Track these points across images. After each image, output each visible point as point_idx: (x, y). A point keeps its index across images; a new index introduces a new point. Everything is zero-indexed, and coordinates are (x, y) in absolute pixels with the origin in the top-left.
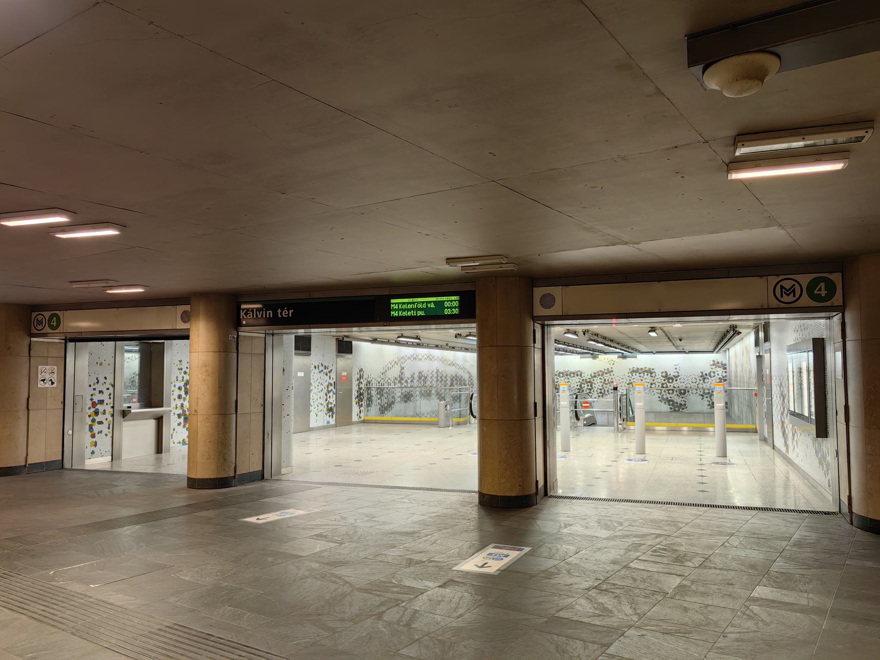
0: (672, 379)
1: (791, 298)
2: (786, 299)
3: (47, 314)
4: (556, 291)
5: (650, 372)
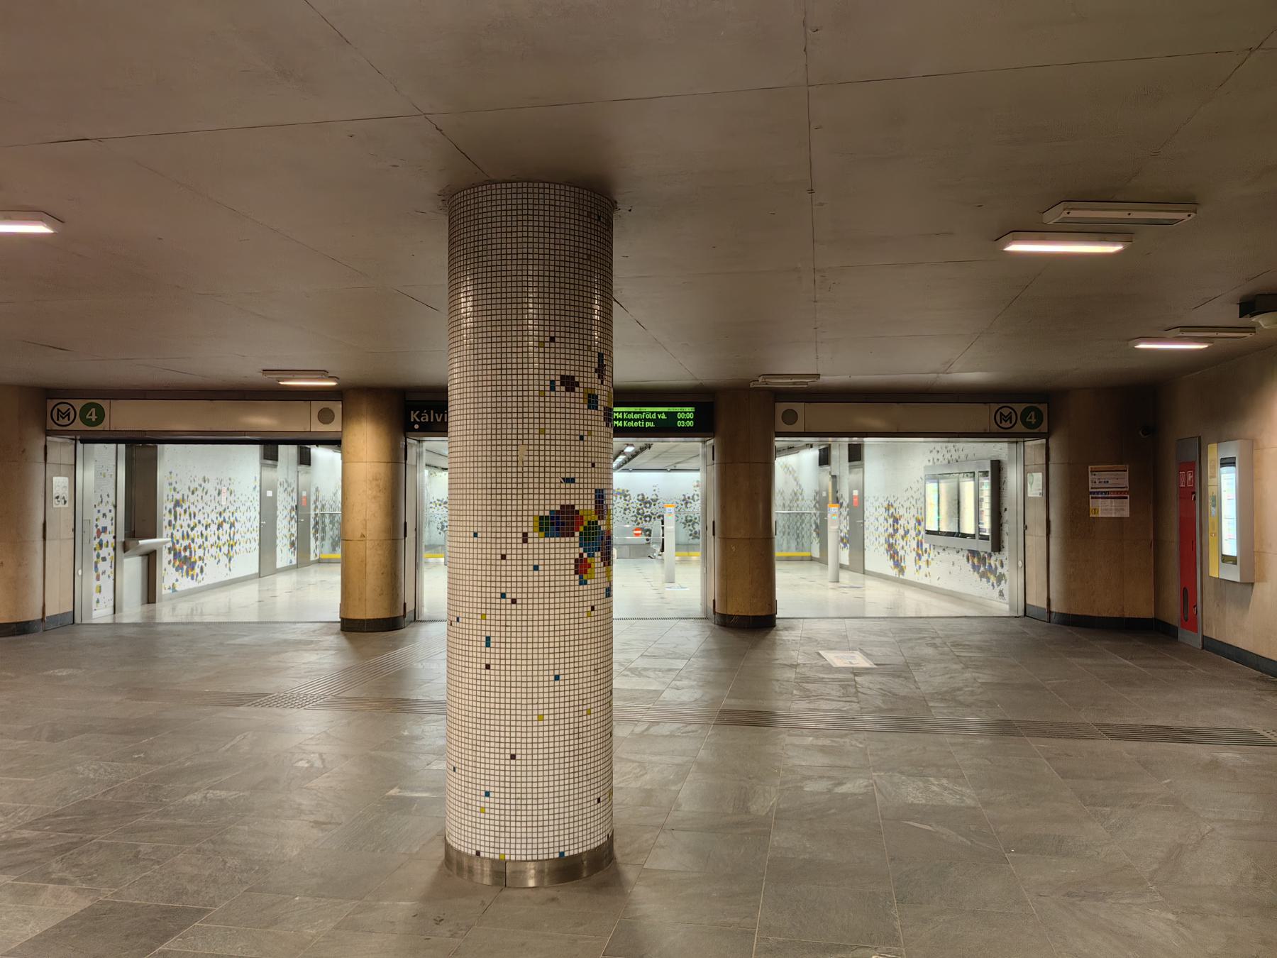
1: (1008, 425)
2: (1004, 425)
3: (79, 404)
4: (799, 407)
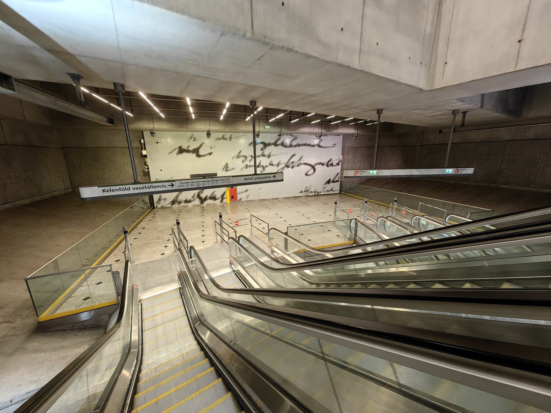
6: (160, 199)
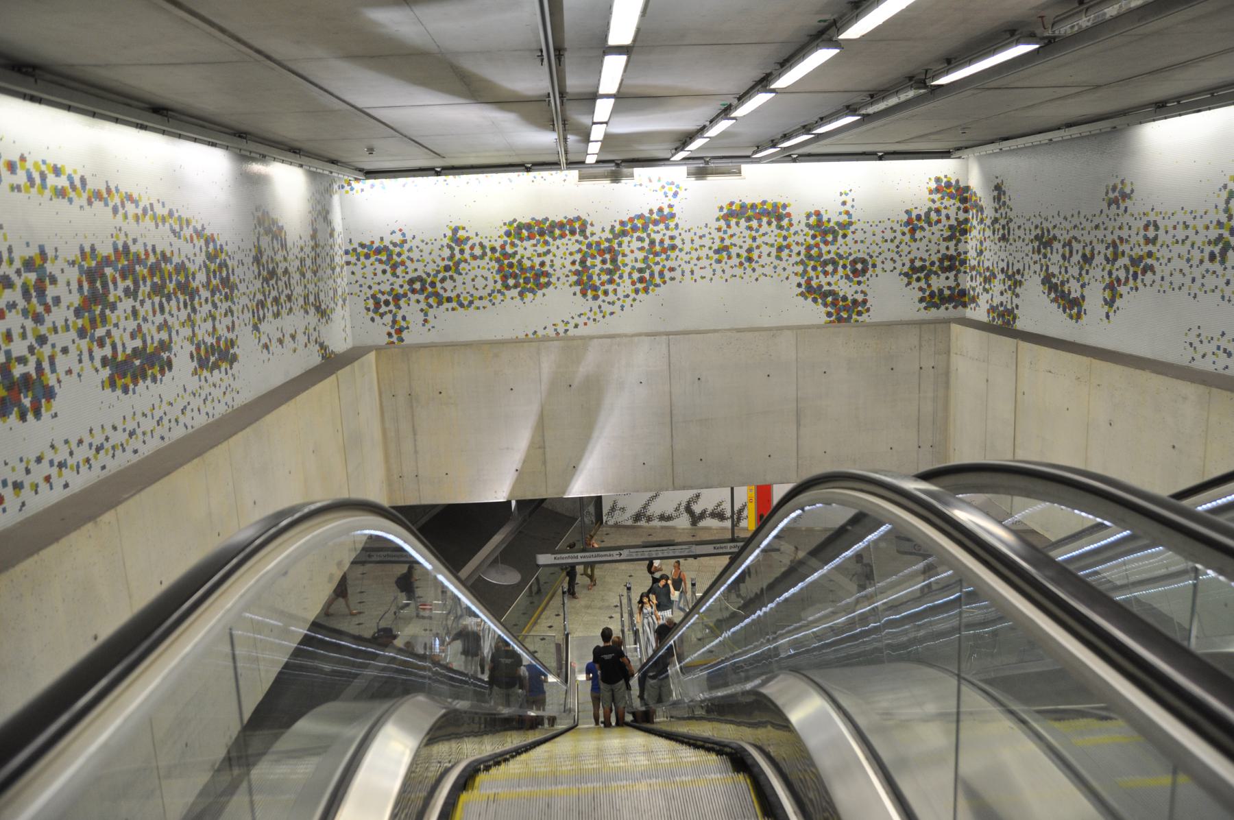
0: (834, 232)
5: (776, 214)
6: (613, 509)
